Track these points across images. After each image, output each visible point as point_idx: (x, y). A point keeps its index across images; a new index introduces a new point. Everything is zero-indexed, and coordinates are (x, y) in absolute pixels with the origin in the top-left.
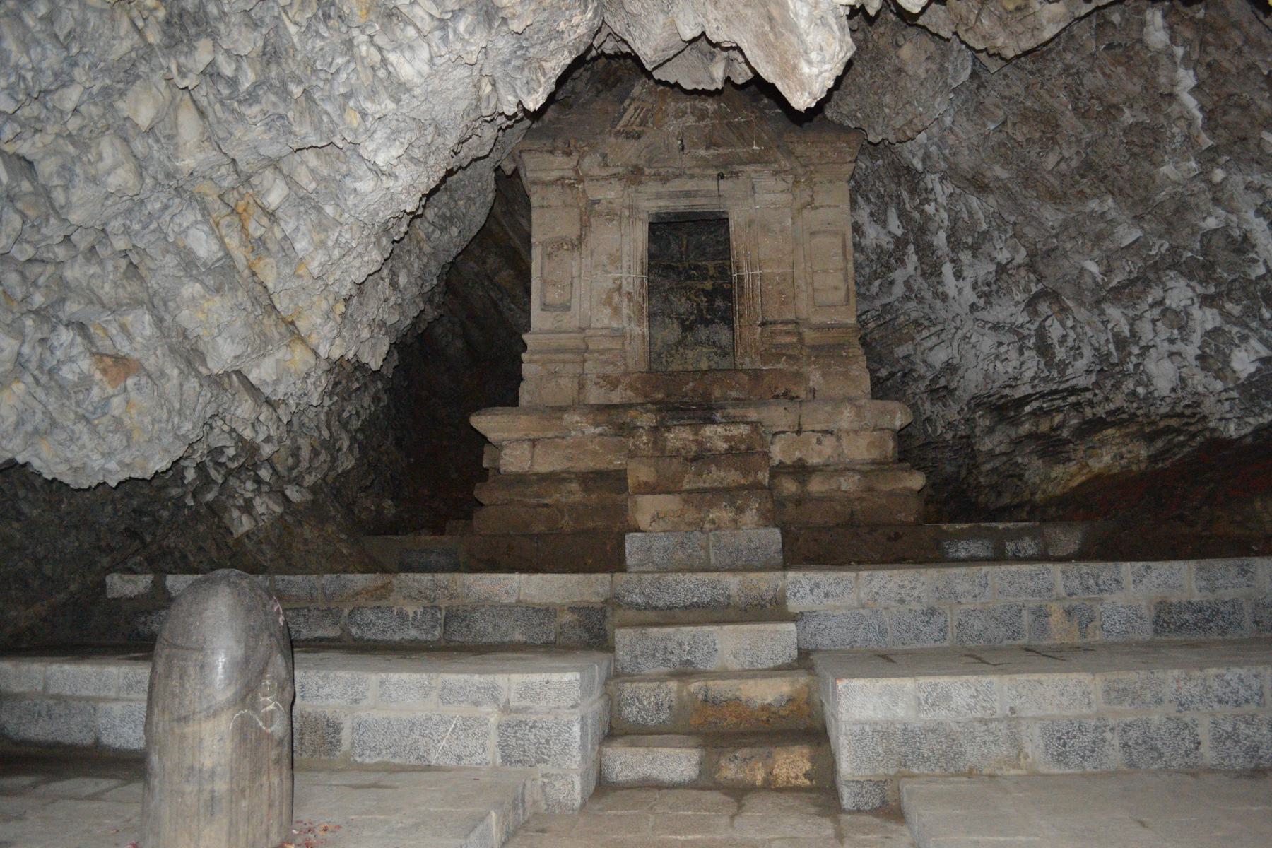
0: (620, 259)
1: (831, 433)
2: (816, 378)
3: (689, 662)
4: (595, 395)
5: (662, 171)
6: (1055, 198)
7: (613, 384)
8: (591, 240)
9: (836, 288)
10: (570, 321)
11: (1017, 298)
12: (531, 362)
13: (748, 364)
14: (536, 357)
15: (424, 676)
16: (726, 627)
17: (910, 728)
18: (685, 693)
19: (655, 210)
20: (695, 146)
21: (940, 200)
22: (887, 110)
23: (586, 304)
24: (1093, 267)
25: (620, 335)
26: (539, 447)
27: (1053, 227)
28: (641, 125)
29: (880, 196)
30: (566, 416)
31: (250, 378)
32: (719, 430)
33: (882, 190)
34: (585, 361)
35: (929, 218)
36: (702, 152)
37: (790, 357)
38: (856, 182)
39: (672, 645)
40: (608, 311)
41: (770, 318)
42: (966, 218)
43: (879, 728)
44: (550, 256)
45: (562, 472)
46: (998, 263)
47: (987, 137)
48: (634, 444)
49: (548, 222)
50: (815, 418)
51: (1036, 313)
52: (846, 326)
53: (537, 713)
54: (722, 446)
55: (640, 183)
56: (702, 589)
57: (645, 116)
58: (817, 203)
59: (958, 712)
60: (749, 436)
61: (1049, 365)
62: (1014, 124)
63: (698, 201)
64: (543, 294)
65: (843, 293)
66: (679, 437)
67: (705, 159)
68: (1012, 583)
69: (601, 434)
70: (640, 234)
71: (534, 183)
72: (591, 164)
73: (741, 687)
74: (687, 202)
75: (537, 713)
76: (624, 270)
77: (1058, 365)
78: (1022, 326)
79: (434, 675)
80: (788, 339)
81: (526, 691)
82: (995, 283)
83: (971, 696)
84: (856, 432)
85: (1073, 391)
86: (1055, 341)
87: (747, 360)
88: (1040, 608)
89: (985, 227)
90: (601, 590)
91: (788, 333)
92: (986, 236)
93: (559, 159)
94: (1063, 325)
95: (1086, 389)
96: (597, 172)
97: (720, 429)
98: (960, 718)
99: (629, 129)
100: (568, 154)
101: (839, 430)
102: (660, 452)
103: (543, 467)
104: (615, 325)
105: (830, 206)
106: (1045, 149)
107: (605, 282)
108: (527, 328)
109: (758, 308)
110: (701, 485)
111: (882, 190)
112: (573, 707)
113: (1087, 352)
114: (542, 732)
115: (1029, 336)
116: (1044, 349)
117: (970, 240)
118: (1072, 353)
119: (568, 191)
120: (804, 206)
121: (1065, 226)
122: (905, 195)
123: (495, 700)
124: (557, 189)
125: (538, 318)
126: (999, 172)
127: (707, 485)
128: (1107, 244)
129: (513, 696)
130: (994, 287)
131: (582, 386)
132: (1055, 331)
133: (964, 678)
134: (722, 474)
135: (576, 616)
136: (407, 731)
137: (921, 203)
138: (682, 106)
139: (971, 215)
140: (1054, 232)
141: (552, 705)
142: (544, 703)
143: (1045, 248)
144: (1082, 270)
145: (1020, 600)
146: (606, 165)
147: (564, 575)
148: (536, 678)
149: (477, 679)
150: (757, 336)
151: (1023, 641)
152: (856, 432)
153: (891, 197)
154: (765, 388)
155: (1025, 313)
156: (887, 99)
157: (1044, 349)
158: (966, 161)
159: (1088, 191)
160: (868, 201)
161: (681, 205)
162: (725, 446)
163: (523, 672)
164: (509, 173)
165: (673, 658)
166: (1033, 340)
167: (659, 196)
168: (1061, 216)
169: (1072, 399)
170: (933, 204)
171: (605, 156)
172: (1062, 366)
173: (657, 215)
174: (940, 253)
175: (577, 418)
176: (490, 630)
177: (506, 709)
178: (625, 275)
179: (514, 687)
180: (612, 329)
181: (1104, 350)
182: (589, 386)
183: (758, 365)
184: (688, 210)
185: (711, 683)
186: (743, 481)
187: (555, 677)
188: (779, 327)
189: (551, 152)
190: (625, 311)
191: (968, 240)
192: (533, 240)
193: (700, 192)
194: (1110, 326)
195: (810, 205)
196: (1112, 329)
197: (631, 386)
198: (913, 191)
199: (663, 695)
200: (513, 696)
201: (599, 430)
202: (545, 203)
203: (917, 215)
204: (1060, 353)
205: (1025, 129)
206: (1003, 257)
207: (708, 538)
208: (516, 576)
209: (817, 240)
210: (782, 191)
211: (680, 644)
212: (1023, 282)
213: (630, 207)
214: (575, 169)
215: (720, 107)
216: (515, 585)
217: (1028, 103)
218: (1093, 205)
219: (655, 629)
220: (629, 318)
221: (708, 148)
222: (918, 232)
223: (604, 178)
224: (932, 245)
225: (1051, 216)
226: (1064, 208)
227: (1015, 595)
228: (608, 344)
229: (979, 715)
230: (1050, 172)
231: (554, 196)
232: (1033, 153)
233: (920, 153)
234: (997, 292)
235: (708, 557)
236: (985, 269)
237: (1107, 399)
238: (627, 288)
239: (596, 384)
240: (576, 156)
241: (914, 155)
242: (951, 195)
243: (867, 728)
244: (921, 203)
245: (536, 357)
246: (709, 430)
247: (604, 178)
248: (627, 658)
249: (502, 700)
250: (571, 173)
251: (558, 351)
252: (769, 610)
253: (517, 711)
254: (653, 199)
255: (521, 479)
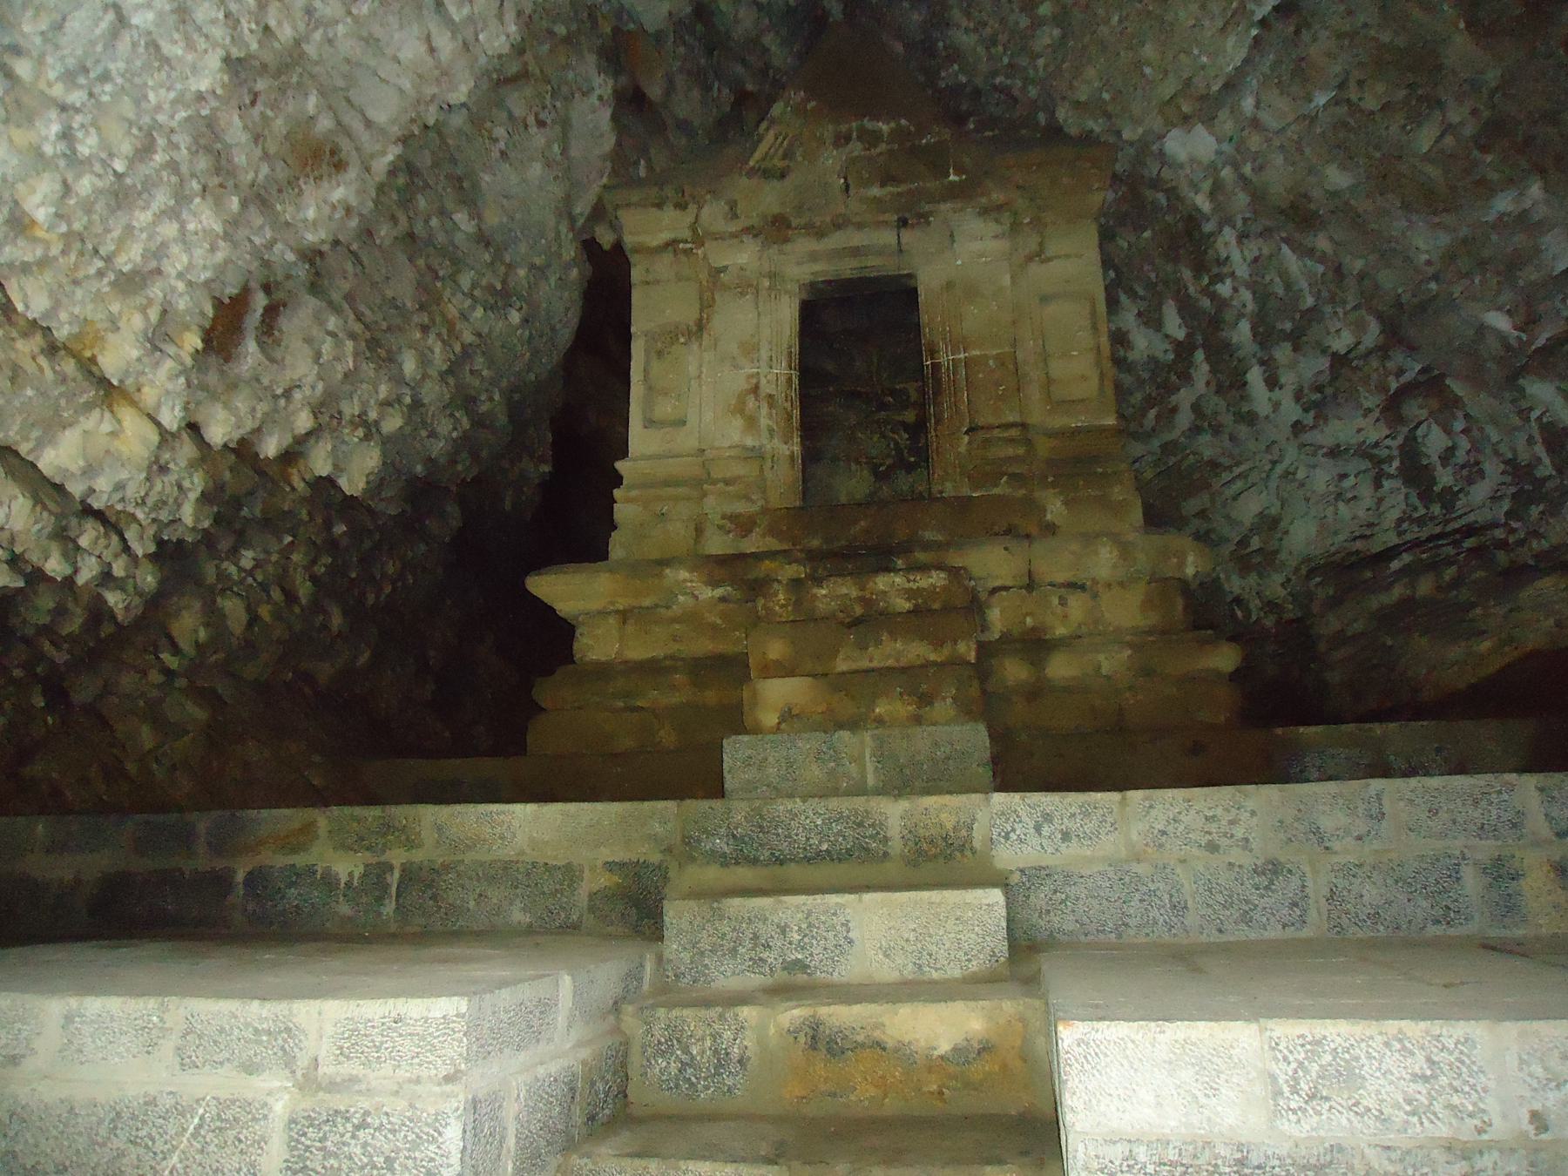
0: (756, 348)
1: (1083, 587)
2: (1055, 509)
3: (801, 966)
4: (717, 544)
5: (817, 221)
6: (1431, 202)
7: (743, 525)
8: (717, 323)
9: (1084, 378)
10: (686, 440)
11: (1367, 404)
12: (628, 500)
13: (949, 490)
14: (634, 493)
15: (152, 1003)
16: (868, 897)
17: (1255, 1159)
18: (772, 1031)
19: (808, 278)
20: (867, 184)
21: (1239, 273)
22: (1148, 70)
23: (708, 416)
24: (1500, 321)
25: (755, 455)
26: (631, 621)
27: (1429, 263)
28: (785, 156)
29: (1150, 286)
30: (668, 571)
31: (40, 466)
32: (898, 580)
33: (1153, 276)
34: (705, 495)
35: (1221, 304)
36: (876, 191)
37: (1012, 476)
38: (1116, 270)
39: (766, 931)
40: (738, 422)
41: (981, 421)
42: (1280, 291)
43: (1172, 1155)
44: (660, 354)
45: (665, 658)
46: (1335, 355)
47: (1313, 119)
48: (765, 607)
49: (654, 306)
50: (1055, 563)
51: (1401, 420)
52: (1103, 430)
53: (369, 1092)
54: (904, 605)
55: (786, 240)
56: (836, 828)
57: (791, 144)
58: (1049, 254)
59: (1382, 1119)
60: (944, 588)
61: (1426, 496)
62: (1361, 83)
63: (872, 261)
64: (648, 403)
65: (1095, 382)
66: (832, 594)
67: (878, 201)
68: (1433, 812)
69: (723, 599)
70: (787, 313)
71: (636, 250)
72: (712, 214)
73: (885, 1020)
74: (854, 263)
75: (369, 1092)
76: (763, 364)
77: (1441, 495)
78: (1377, 445)
79: (172, 1002)
80: (1010, 451)
81: (352, 1042)
82: (1330, 383)
83: (1416, 1077)
84: (1121, 584)
85: (1470, 530)
86: (1435, 459)
87: (949, 485)
88: (1498, 861)
89: (1310, 301)
90: (658, 828)
91: (1011, 440)
92: (1313, 315)
93: (669, 215)
94: (1448, 431)
95: (1495, 525)
96: (721, 225)
97: (899, 580)
98: (1391, 1138)
99: (767, 164)
100: (681, 206)
101: (1095, 581)
102: (805, 618)
103: (637, 653)
104: (749, 442)
105: (1068, 256)
106: (1416, 119)
107: (737, 381)
108: (624, 453)
109: (963, 408)
110: (865, 664)
111: (1153, 276)
112: (448, 1079)
113: (1493, 468)
114: (379, 1140)
115: (1390, 459)
116: (1416, 473)
117: (1288, 326)
118: (1465, 472)
119: (683, 258)
120: (1030, 259)
121: (1450, 257)
122: (1187, 274)
123: (289, 1061)
124: (668, 257)
125: (639, 438)
126: (1337, 178)
127: (875, 664)
128: (1530, 275)
129: (325, 1050)
130: (1329, 391)
131: (699, 531)
132: (1434, 441)
133: (1392, 1026)
134: (898, 645)
135: (616, 879)
136: (103, 1132)
137: (1210, 283)
138: (844, 128)
139: (1288, 286)
140: (1431, 270)
141: (402, 1074)
142: (387, 1069)
143: (1415, 300)
144: (1482, 329)
145: (1456, 845)
146: (735, 216)
147: (599, 806)
148: (374, 1010)
149: (258, 1012)
150: (962, 449)
151: (1472, 928)
152: (1121, 584)
153: (1166, 283)
154: (969, 521)
155: (1381, 424)
156: (1149, 51)
157: (1416, 473)
158: (1278, 177)
159: (1495, 176)
160: (1133, 294)
161: (847, 268)
162: (907, 606)
163: (396, 995)
164: (607, 247)
165: (770, 957)
166: (1396, 464)
167: (813, 257)
168: (1444, 239)
169: (1469, 543)
170: (1228, 281)
171: (733, 205)
172: (1448, 498)
173: (812, 284)
174: (1241, 354)
175: (684, 574)
176: (472, 904)
177: (309, 1082)
178: (764, 370)
179: (329, 1029)
180: (745, 448)
181: (1524, 457)
182: (710, 531)
183: (966, 491)
184: (856, 274)
185: (823, 1011)
186: (932, 657)
187: (414, 1008)
188: (996, 432)
189: (659, 206)
190: (764, 422)
191: (1286, 324)
192: (633, 329)
193: (869, 246)
194: (1535, 415)
195: (1039, 255)
196: (1539, 418)
197: (772, 531)
198: (1199, 268)
199: (728, 1034)
200: (325, 1050)
201: (719, 592)
202: (650, 278)
203: (1206, 303)
204: (1445, 478)
205: (1380, 88)
206: (1342, 342)
207: (862, 742)
208: (519, 809)
209: (1052, 309)
210: (996, 237)
211: (783, 930)
212: (1375, 376)
213: (772, 276)
214: (693, 228)
215: (898, 124)
216: (516, 823)
217: (1386, 37)
218: (1504, 203)
219: (737, 901)
220: (771, 431)
221: (883, 185)
222: (1208, 328)
223: (734, 235)
224: (1229, 345)
225: (1427, 242)
226: (1447, 219)
227: (1443, 835)
228: (738, 470)
229: (1443, 1131)
230: (1426, 158)
231: (664, 266)
232: (1394, 129)
233: (1207, 186)
234: (1335, 396)
235: (864, 777)
236: (1314, 366)
237: (1536, 534)
238: (766, 388)
239: (720, 527)
240: (692, 208)
241: (1195, 188)
242: (1256, 260)
243: (1142, 1154)
244: (1213, 282)
245: (634, 493)
246: (882, 582)
247: (734, 235)
248: (686, 956)
249: (303, 1061)
250: (687, 234)
251: (667, 483)
252: (942, 863)
253: (333, 1086)
254: (804, 262)
255: (603, 671)
